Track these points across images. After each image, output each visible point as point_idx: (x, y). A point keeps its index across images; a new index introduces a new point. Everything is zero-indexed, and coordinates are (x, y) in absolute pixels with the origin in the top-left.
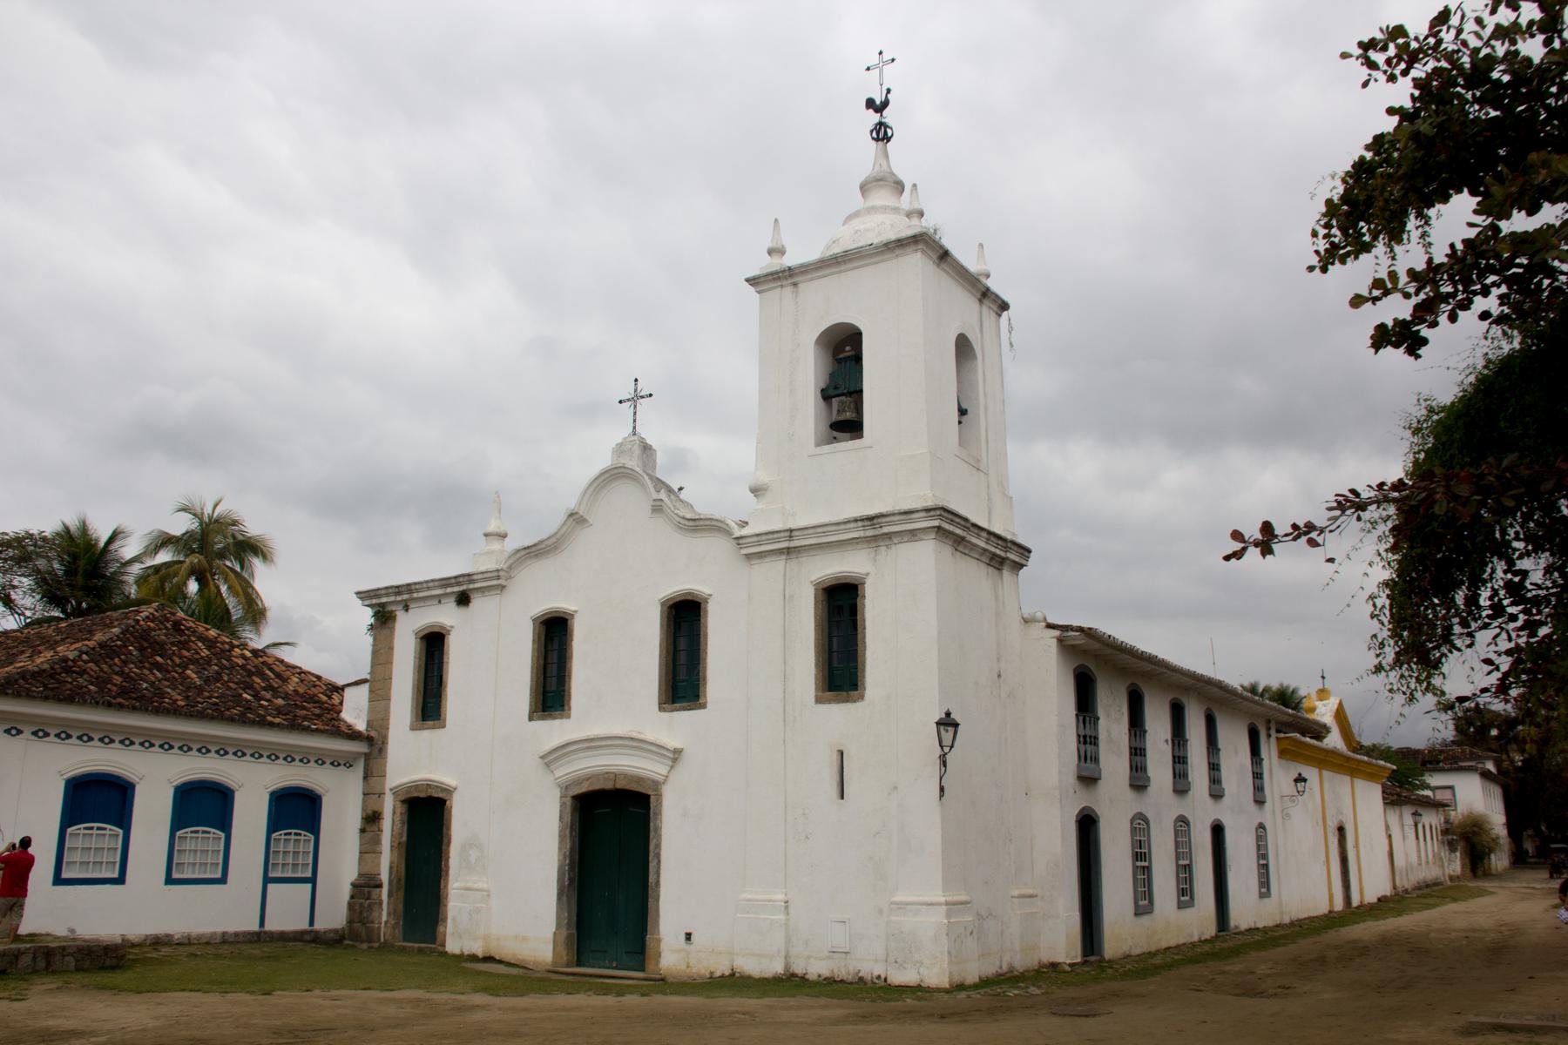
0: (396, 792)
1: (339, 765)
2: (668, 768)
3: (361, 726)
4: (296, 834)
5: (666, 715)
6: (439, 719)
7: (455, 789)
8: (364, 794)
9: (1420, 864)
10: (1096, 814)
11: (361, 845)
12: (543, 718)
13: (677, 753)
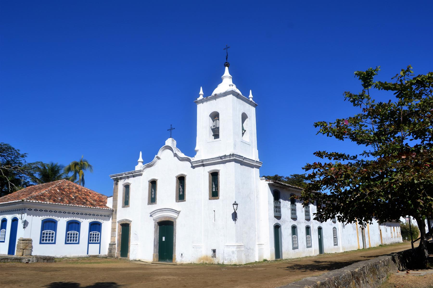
1: (106, 216)
2: (177, 215)
4: (96, 232)
5: (177, 203)
6: (128, 205)
7: (132, 221)
8: (112, 223)
9: (392, 237)
10: (310, 226)
11: (111, 235)
12: (150, 204)
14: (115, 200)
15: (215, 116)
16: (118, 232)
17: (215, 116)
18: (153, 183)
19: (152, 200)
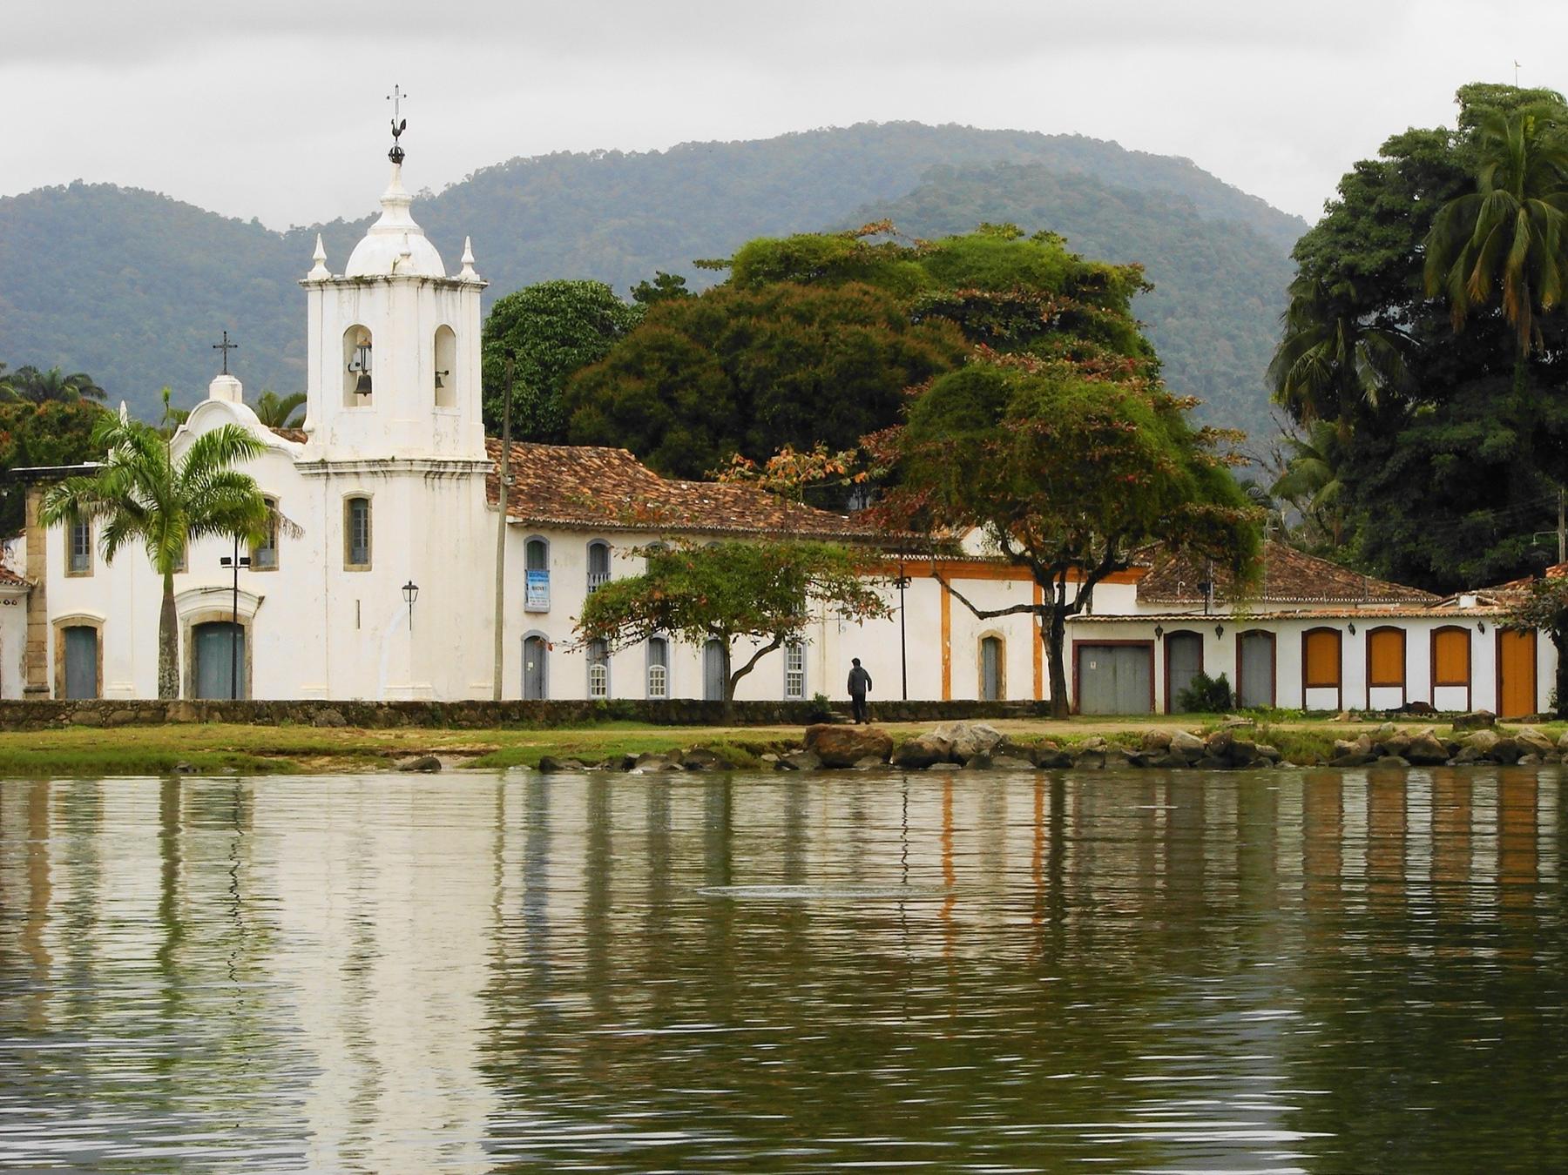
0: (55, 622)
3: (20, 571)
13: (261, 599)
14: (36, 550)
15: (359, 339)
16: (56, 653)
17: (359, 339)
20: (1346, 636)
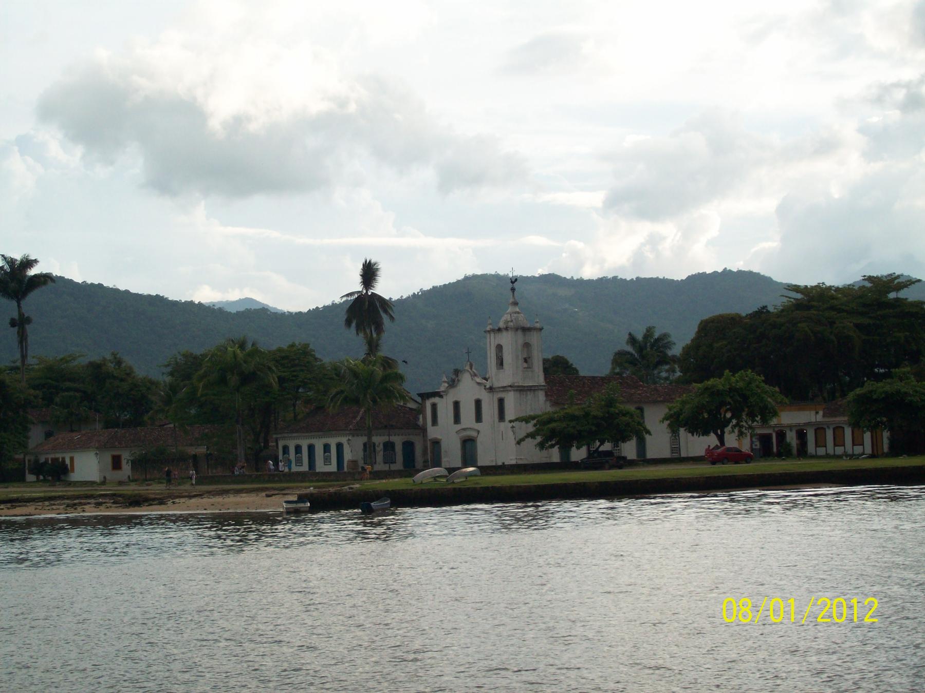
14: (425, 418)
15: (499, 348)
17: (499, 348)
18: (456, 405)
19: (457, 419)
20: (827, 430)
